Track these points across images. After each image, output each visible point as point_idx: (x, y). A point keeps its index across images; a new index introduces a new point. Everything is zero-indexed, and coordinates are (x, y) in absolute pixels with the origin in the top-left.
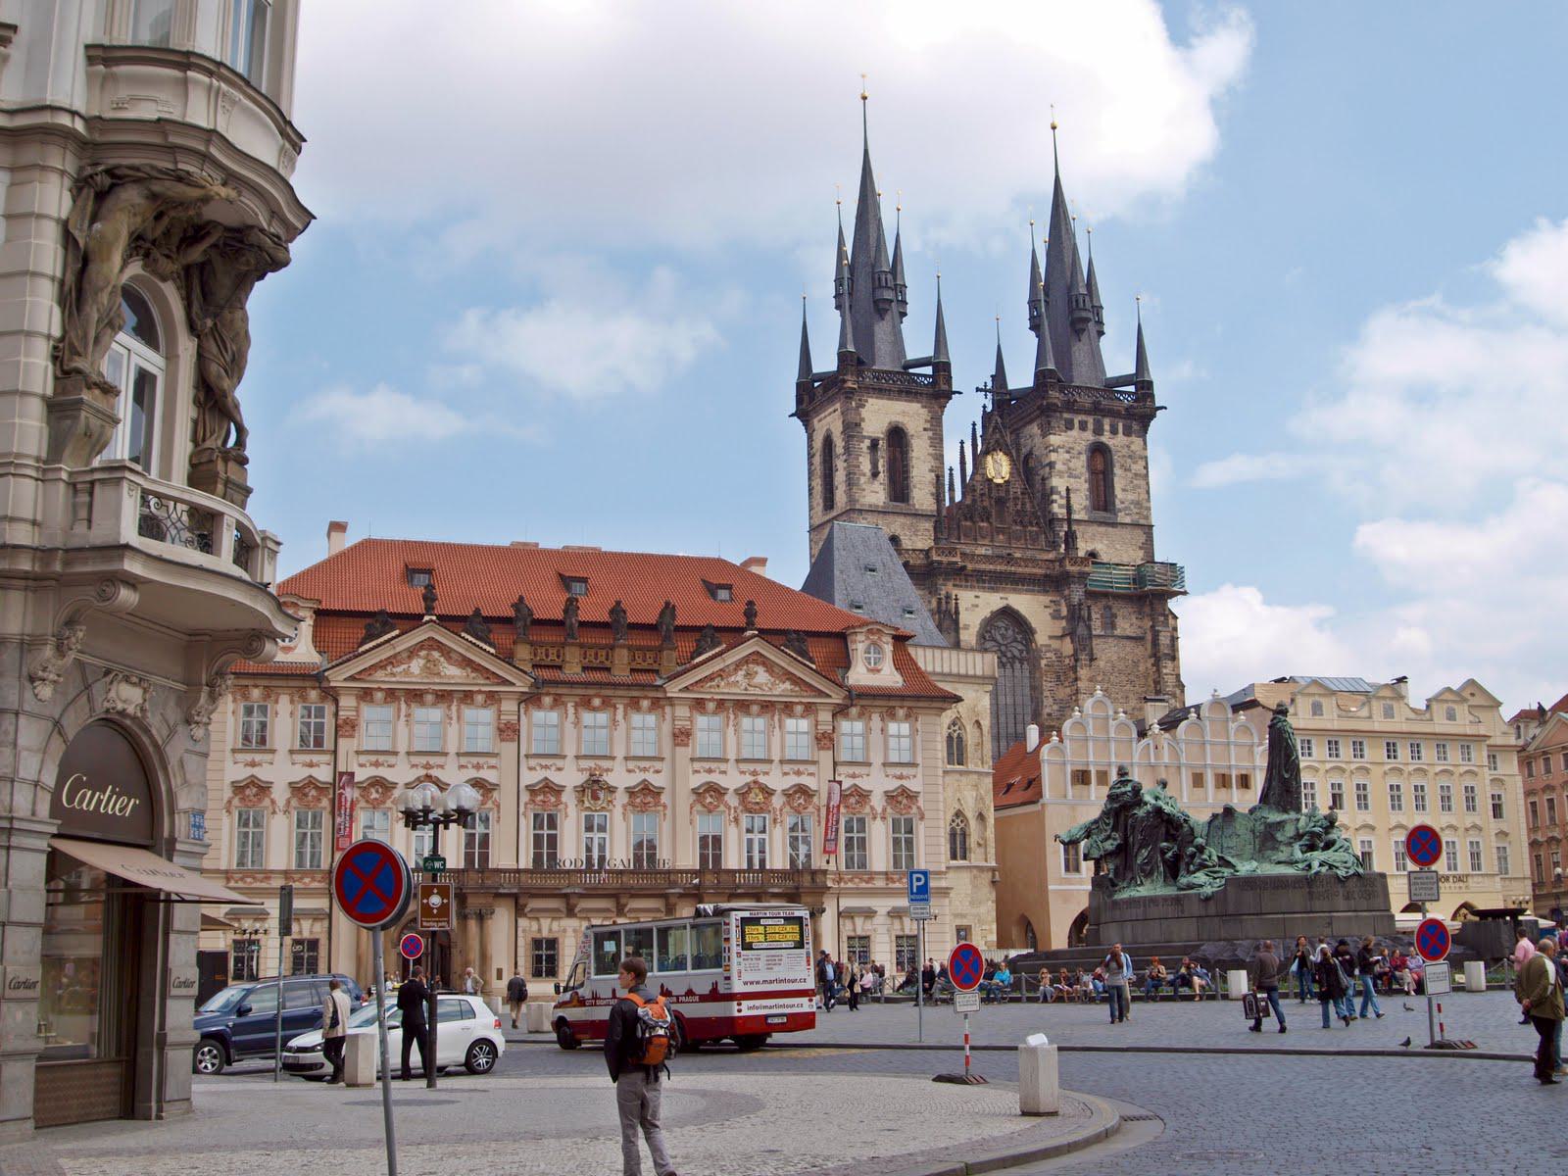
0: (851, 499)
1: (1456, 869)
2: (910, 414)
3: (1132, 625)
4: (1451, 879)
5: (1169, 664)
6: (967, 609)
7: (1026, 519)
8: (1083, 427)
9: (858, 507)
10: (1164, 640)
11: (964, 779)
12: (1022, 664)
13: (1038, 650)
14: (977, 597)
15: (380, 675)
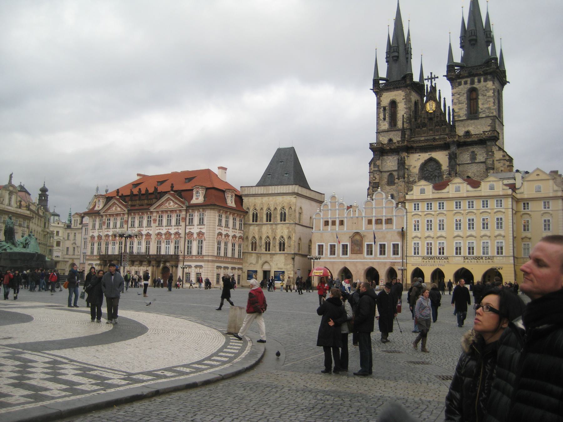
0: (377, 129)
1: (487, 254)
2: (399, 95)
3: (484, 157)
4: (484, 258)
5: (492, 171)
6: (415, 161)
7: (440, 124)
8: (466, 83)
9: (379, 131)
10: (489, 162)
11: (284, 226)
12: (438, 177)
13: (444, 172)
14: (419, 156)
15: (109, 211)
